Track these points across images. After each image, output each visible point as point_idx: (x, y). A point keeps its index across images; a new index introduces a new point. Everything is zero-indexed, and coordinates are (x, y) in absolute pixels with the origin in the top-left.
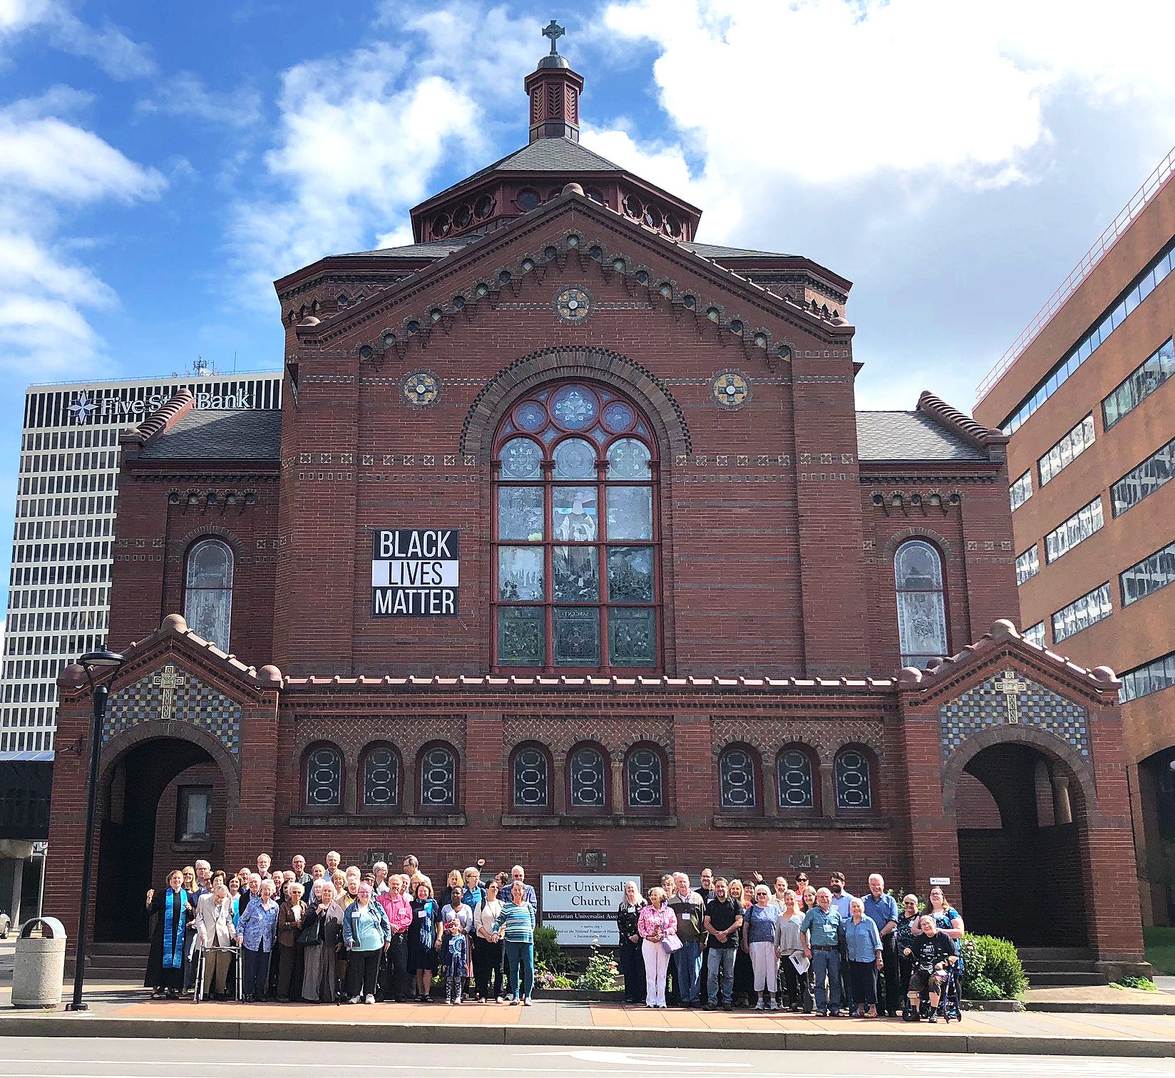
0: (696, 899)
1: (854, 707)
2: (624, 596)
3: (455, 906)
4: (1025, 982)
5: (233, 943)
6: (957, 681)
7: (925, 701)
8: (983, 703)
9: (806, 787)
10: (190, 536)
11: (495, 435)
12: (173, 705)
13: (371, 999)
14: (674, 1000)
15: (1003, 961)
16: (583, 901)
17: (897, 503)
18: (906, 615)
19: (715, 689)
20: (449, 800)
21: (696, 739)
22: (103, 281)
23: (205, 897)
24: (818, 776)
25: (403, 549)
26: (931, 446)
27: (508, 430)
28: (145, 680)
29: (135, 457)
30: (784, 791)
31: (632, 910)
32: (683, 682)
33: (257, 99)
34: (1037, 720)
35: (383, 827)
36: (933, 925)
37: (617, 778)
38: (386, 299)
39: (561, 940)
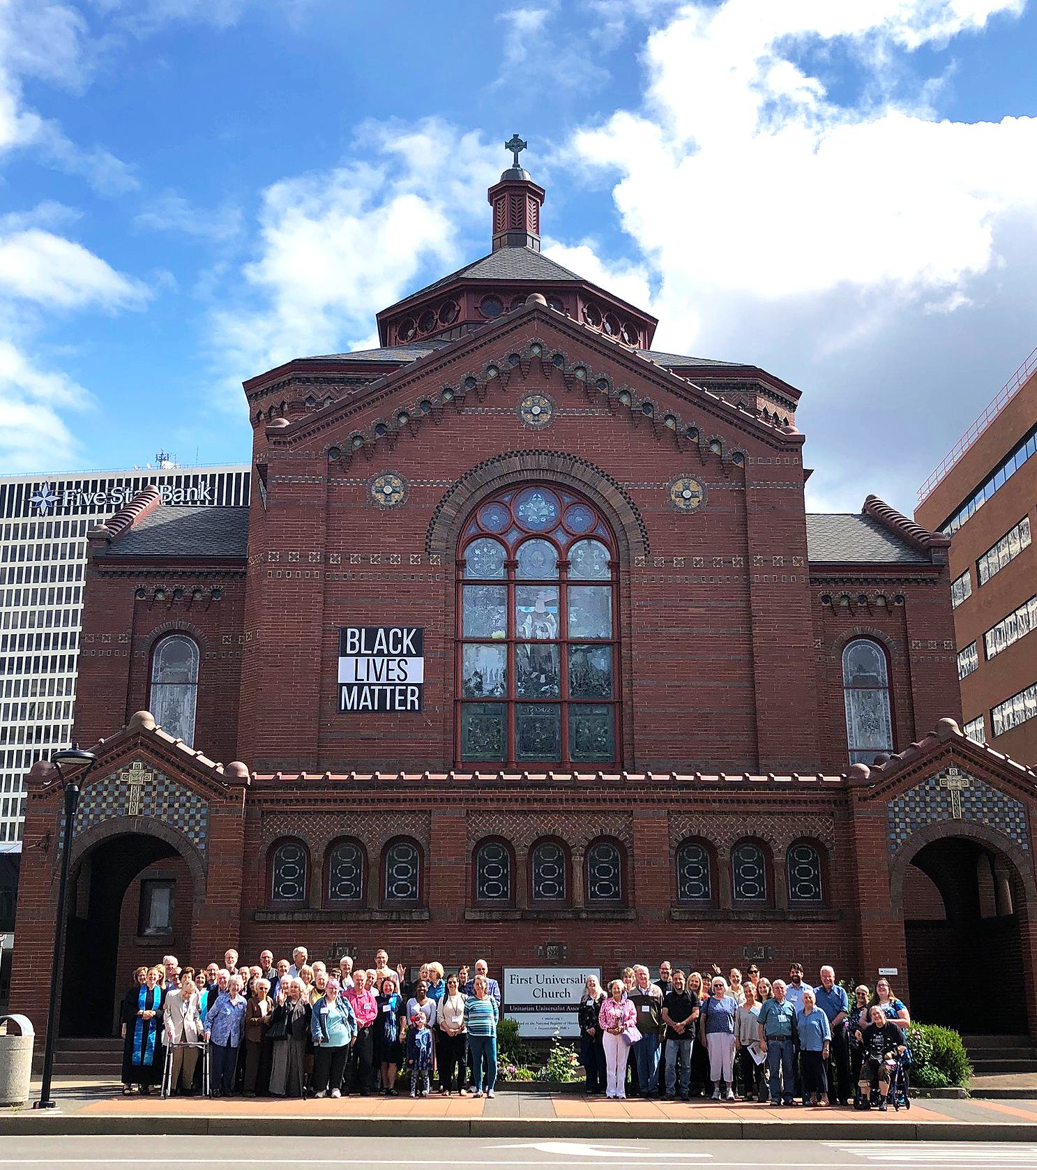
0: (655, 991)
1: (805, 802)
2: (587, 693)
3: (420, 999)
4: (970, 1072)
5: (200, 1038)
6: (904, 777)
7: (873, 796)
8: (928, 799)
9: (760, 879)
10: (157, 631)
11: (459, 536)
12: (141, 800)
13: (337, 1093)
14: (634, 1091)
15: (949, 1050)
16: (544, 994)
17: (845, 603)
18: (853, 711)
19: (673, 784)
20: (413, 895)
21: (654, 834)
22: (83, 386)
23: (172, 993)
24: (771, 869)
25: (369, 645)
26: (876, 548)
27: (473, 530)
28: (113, 777)
29: (102, 554)
30: (739, 884)
31: (590, 1003)
32: (642, 777)
33: (237, 214)
34: (979, 815)
35: (347, 921)
36: (883, 1015)
37: (578, 871)
38: (353, 402)
39: (523, 1032)
